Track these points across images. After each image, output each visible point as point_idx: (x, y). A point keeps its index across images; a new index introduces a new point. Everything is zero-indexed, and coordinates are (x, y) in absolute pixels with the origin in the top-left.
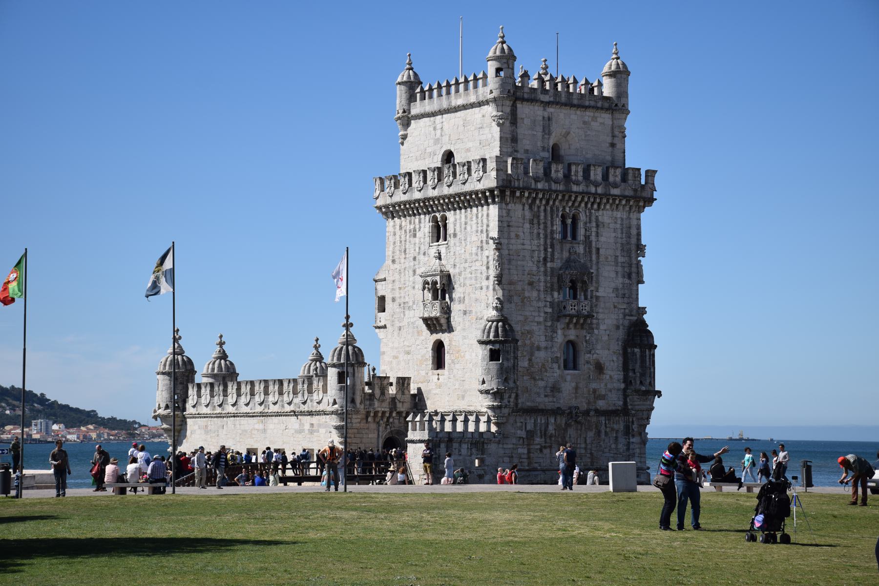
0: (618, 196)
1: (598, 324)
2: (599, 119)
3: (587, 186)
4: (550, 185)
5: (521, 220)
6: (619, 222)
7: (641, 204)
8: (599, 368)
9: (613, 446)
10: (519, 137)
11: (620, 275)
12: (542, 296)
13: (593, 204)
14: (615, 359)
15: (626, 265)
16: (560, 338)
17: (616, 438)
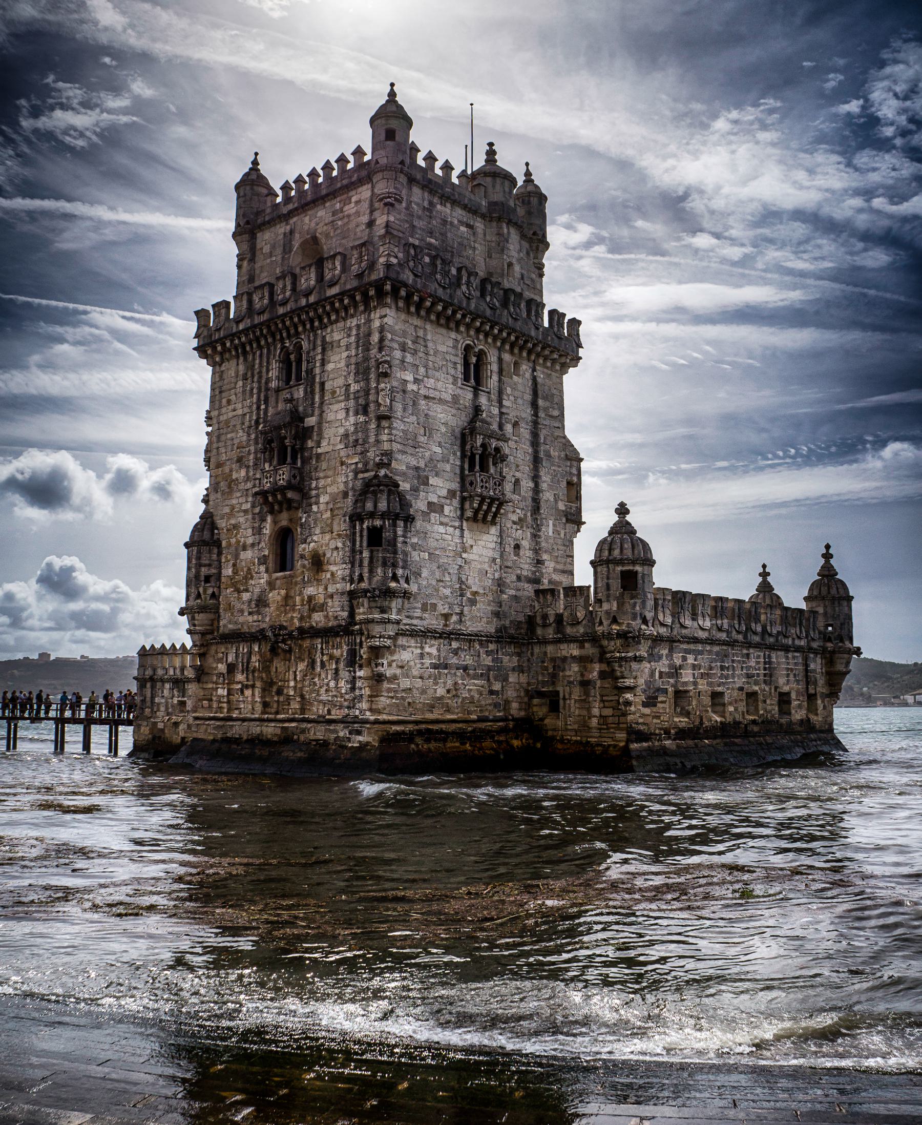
0: (334, 296)
1: (318, 496)
2: (353, 199)
3: (296, 301)
4: (252, 320)
5: (233, 380)
6: (354, 332)
7: (372, 293)
8: (318, 562)
9: (332, 684)
10: (257, 272)
11: (351, 413)
12: (251, 474)
13: (312, 321)
14: (340, 545)
15: (362, 394)
16: (268, 528)
17: (337, 670)
